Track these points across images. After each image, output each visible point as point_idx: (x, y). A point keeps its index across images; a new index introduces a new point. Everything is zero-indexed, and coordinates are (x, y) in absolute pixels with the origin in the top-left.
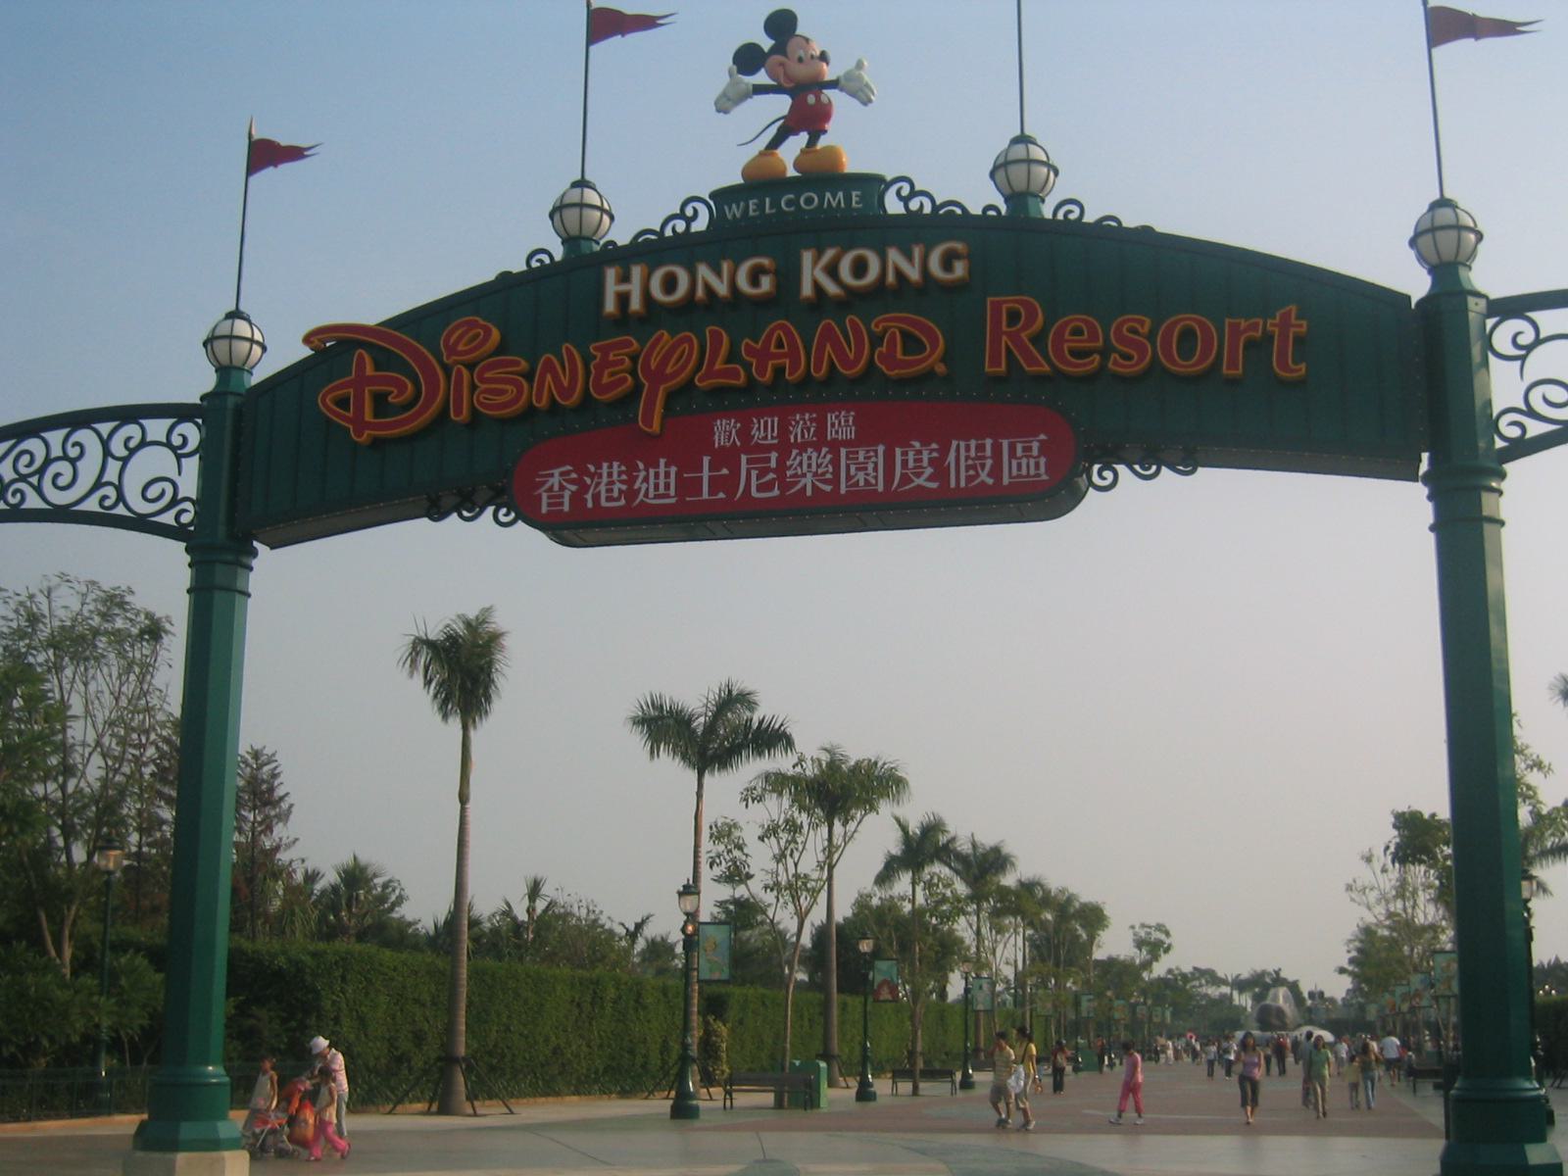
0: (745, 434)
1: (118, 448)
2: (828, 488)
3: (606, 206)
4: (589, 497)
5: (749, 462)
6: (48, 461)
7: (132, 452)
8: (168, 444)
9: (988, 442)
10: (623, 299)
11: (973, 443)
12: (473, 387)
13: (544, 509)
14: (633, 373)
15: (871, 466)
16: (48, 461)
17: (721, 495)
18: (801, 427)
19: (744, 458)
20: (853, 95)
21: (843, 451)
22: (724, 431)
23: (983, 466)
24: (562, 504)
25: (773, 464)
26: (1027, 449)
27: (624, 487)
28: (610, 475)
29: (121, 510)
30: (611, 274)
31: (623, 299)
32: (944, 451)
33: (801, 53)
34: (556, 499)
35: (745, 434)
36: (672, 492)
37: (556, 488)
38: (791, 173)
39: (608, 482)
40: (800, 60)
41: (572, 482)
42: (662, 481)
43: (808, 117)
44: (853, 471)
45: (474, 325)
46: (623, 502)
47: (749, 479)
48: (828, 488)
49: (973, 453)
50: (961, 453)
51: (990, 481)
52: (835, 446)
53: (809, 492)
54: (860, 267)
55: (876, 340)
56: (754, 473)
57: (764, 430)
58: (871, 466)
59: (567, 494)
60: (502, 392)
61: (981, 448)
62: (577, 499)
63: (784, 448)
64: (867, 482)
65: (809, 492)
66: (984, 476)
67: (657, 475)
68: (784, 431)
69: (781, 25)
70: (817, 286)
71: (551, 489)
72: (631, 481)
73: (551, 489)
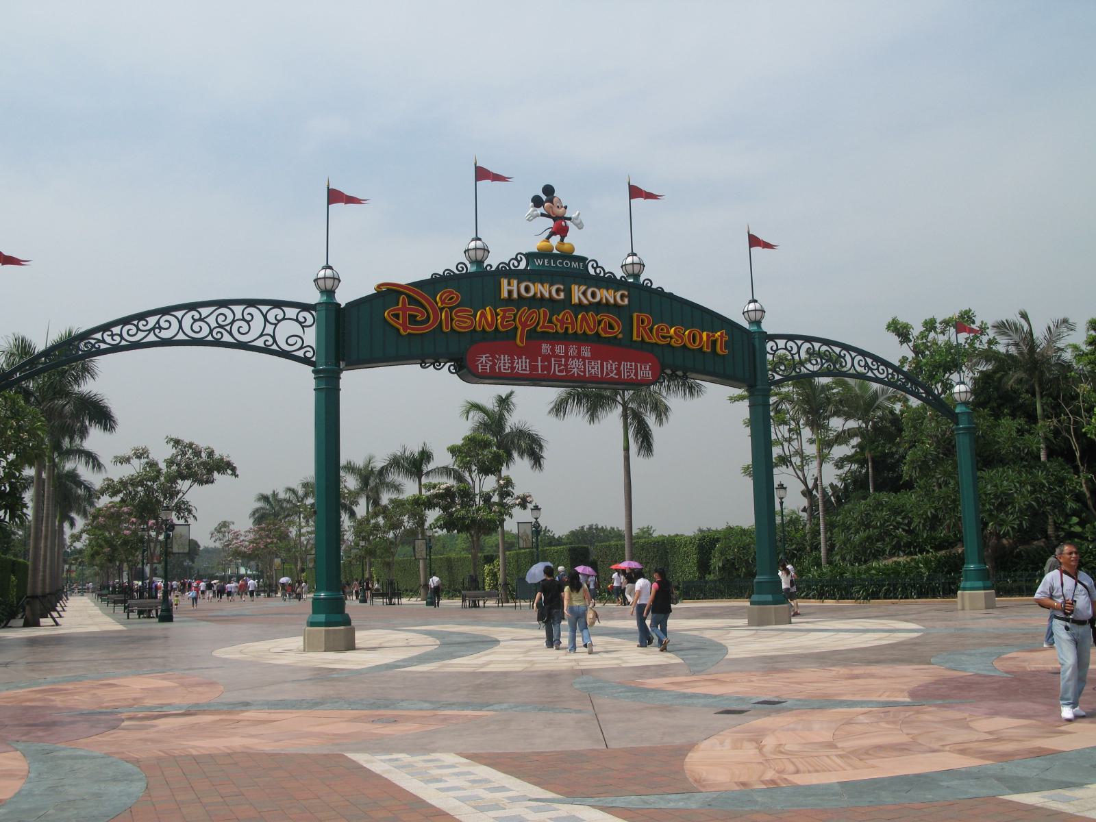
0: (553, 350)
1: (271, 317)
2: (582, 374)
3: (486, 248)
4: (497, 367)
5: (555, 361)
6: (234, 321)
7: (279, 321)
8: (297, 320)
9: (633, 364)
10: (510, 292)
11: (629, 364)
12: (452, 320)
13: (480, 371)
14: (514, 320)
15: (596, 367)
16: (234, 321)
17: (545, 372)
18: (572, 350)
19: (553, 359)
20: (576, 225)
21: (587, 361)
22: (545, 348)
23: (632, 372)
24: (486, 369)
25: (563, 363)
26: (645, 368)
27: (510, 365)
28: (504, 360)
29: (274, 347)
30: (504, 282)
31: (510, 292)
32: (620, 365)
33: (558, 204)
34: (484, 367)
35: (553, 350)
36: (528, 369)
37: (484, 362)
38: (555, 251)
39: (504, 363)
40: (558, 207)
41: (490, 361)
42: (524, 364)
43: (561, 231)
44: (590, 369)
45: (451, 293)
46: (509, 371)
47: (555, 368)
48: (582, 374)
49: (629, 367)
50: (625, 366)
51: (634, 378)
52: (584, 359)
53: (576, 375)
54: (594, 295)
55: (600, 322)
56: (557, 365)
57: (560, 349)
58: (596, 367)
59: (488, 365)
60: (466, 322)
61: (631, 365)
62: (492, 367)
63: (567, 357)
64: (595, 373)
65: (576, 375)
66: (632, 375)
67: (522, 362)
68: (566, 352)
69: (549, 190)
70: (579, 299)
71: (482, 363)
72: (512, 363)
73: (482, 363)
